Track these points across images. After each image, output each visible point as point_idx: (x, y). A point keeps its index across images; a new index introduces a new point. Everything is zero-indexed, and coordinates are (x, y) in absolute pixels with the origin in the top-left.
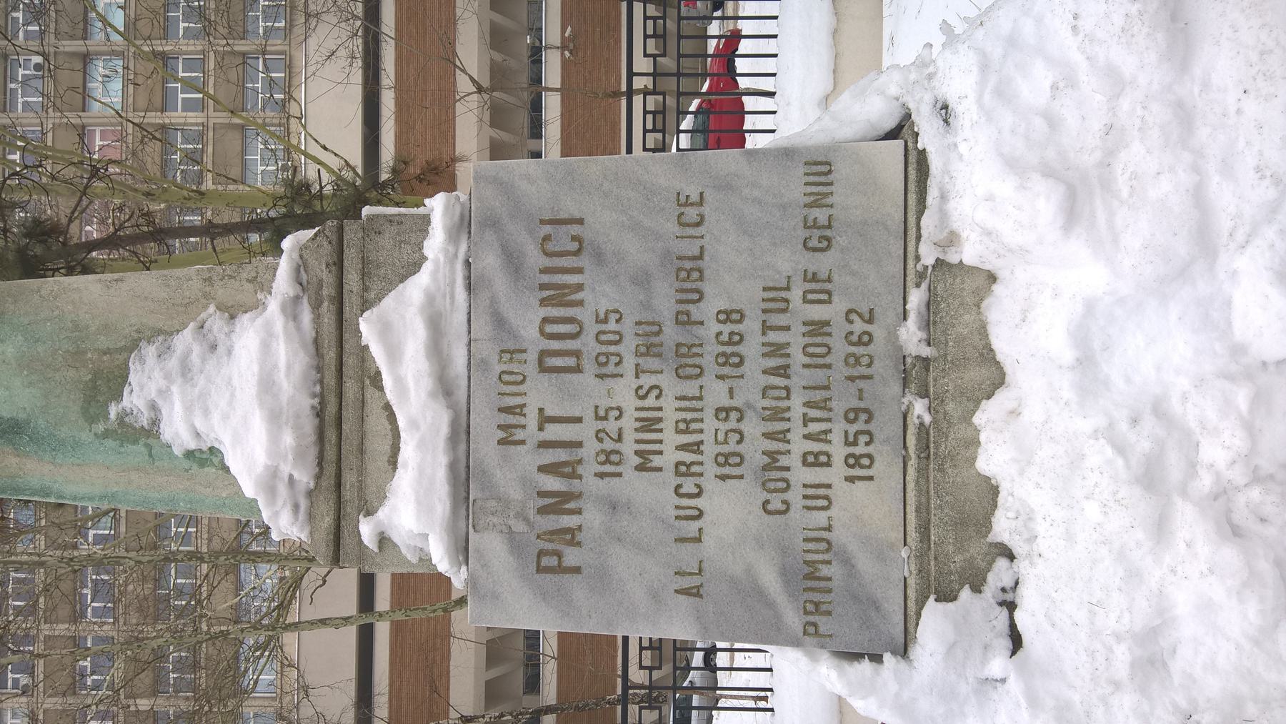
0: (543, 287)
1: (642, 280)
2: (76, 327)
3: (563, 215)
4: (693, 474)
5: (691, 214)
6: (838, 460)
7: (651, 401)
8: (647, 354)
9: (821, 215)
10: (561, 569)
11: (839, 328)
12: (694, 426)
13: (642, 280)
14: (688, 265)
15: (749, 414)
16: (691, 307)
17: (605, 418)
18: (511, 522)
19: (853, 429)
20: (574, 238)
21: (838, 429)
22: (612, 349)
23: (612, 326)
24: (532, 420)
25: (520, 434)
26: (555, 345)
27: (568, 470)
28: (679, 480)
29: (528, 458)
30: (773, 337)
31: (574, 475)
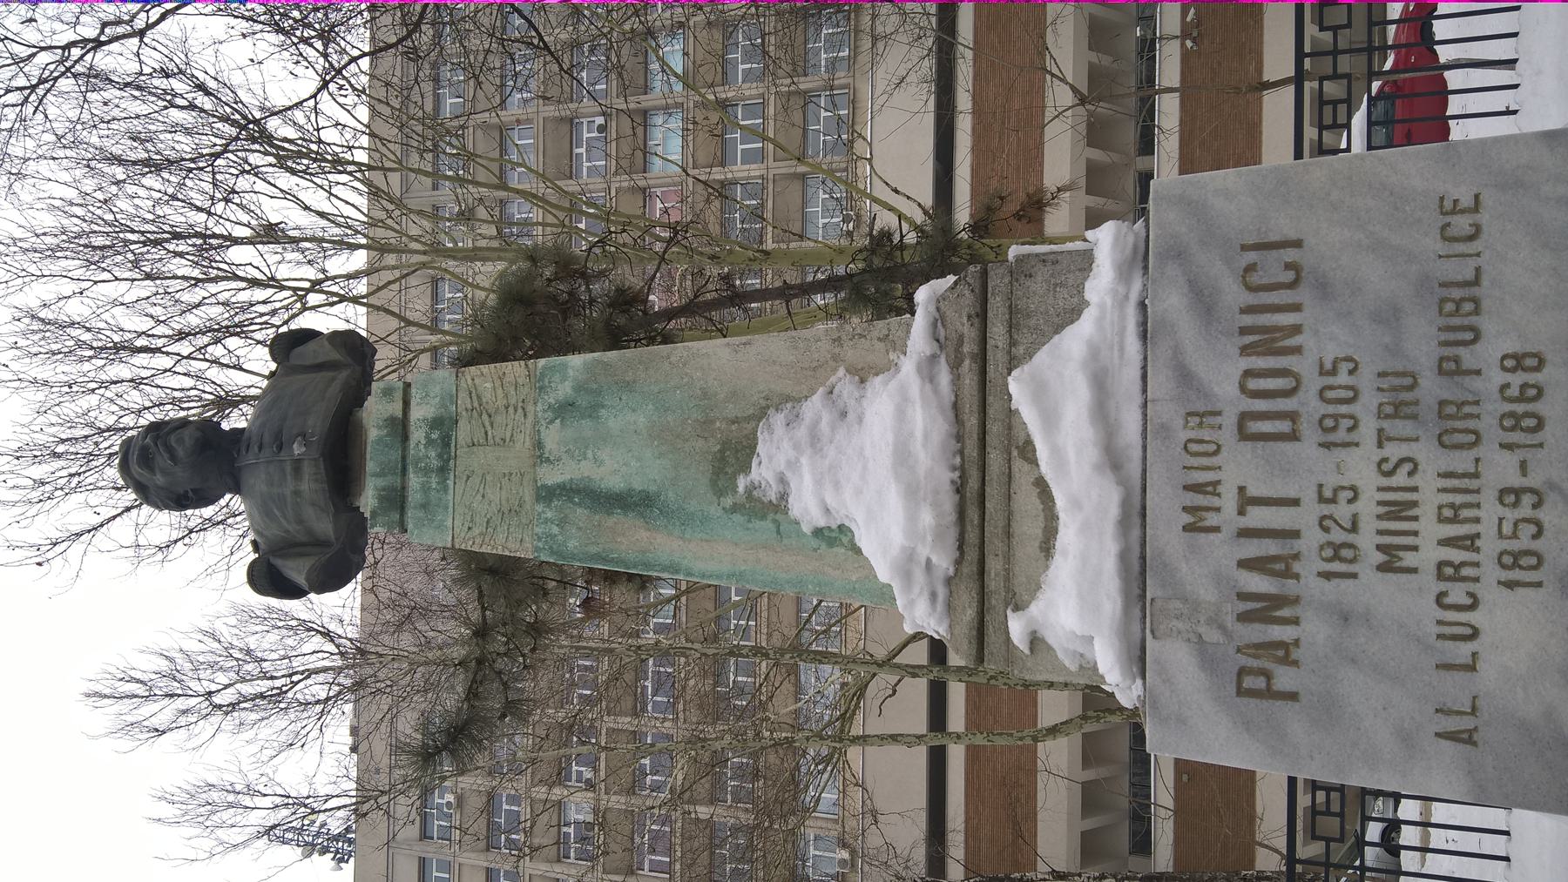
0: (1244, 331)
1: (1389, 316)
2: (705, 394)
3: (1274, 237)
4: (1464, 579)
5: (1462, 224)
7: (1400, 479)
8: (1395, 416)
10: (1270, 694)
12: (1465, 513)
13: (1389, 316)
14: (1457, 293)
15: (1551, 498)
16: (1462, 351)
17: (1333, 501)
18: (1202, 629)
20: (1288, 266)
22: (1343, 409)
23: (1343, 378)
24: (1229, 501)
26: (1261, 405)
27: (1280, 566)
28: (1443, 586)
29: (1223, 551)
31: (1288, 574)
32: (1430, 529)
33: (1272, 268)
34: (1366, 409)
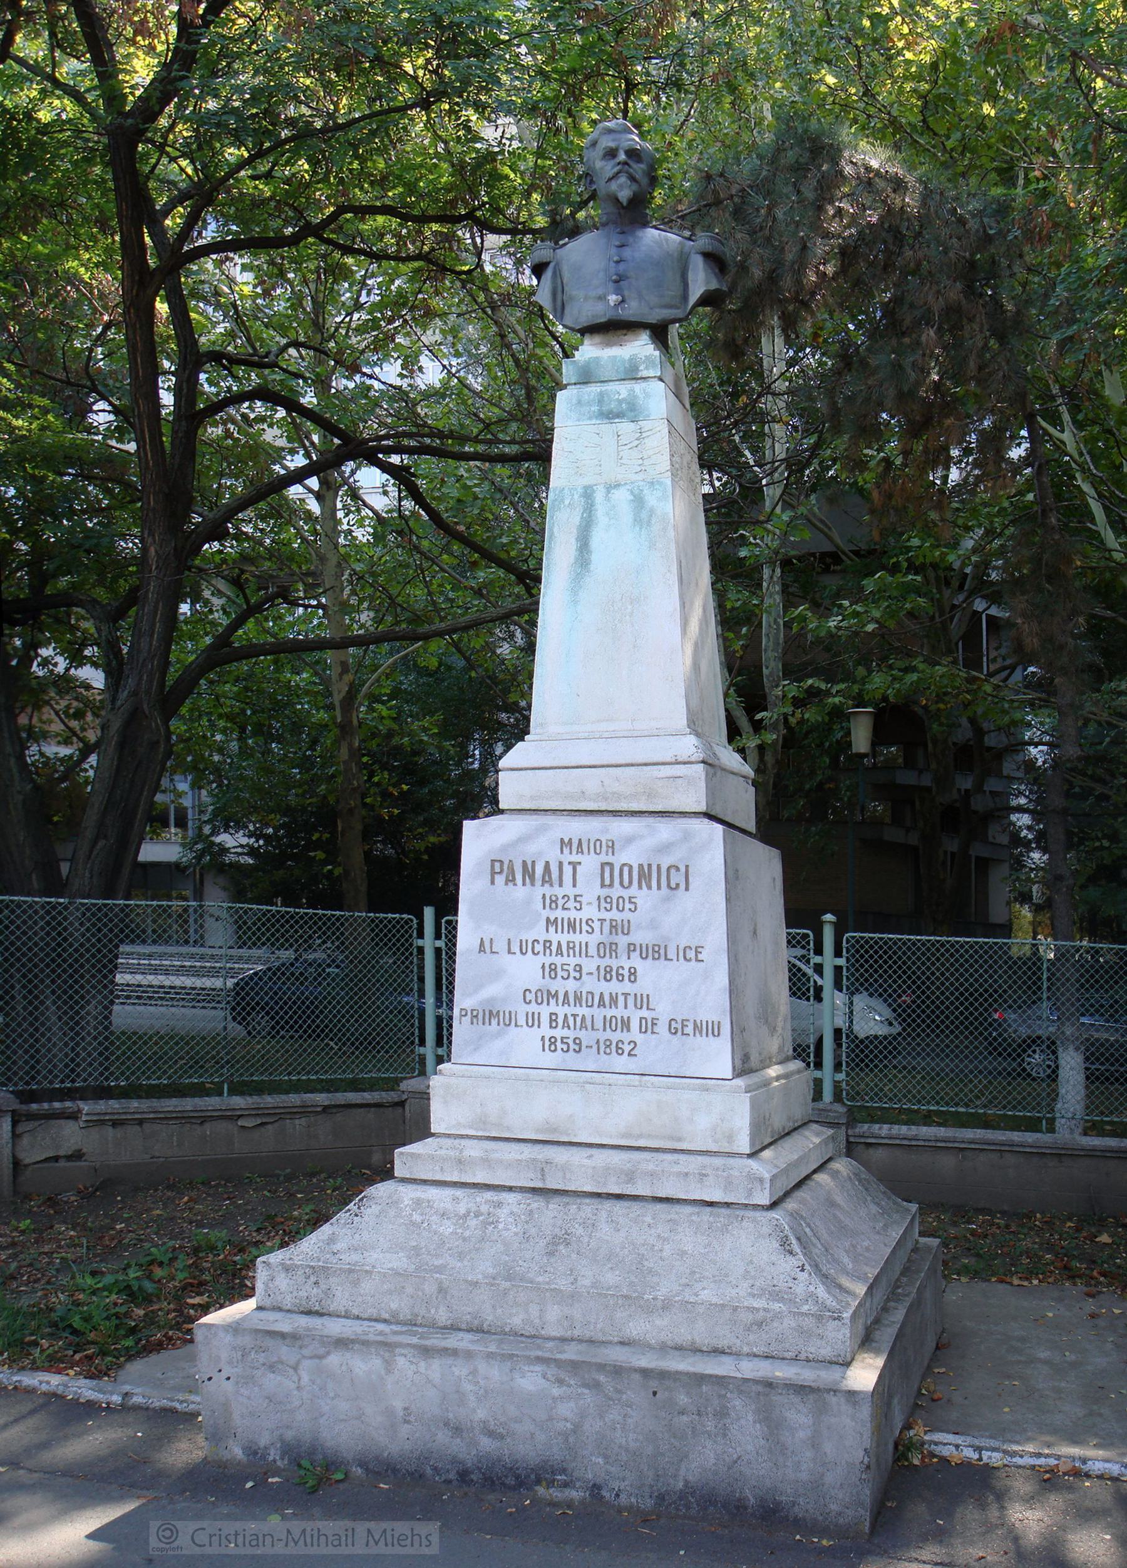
0: (650, 866)
1: (653, 925)
5: (691, 954)
6: (553, 1033)
7: (585, 927)
9: (689, 1029)
10: (493, 873)
11: (626, 1037)
13: (653, 925)
14: (662, 952)
15: (578, 983)
19: (570, 1041)
21: (571, 1034)
23: (628, 906)
24: (575, 858)
25: (566, 850)
29: (553, 855)
30: (621, 999)
31: (544, 882)
32: (565, 938)
33: (677, 878)
34: (614, 914)
